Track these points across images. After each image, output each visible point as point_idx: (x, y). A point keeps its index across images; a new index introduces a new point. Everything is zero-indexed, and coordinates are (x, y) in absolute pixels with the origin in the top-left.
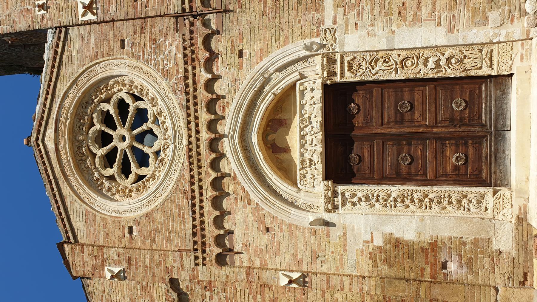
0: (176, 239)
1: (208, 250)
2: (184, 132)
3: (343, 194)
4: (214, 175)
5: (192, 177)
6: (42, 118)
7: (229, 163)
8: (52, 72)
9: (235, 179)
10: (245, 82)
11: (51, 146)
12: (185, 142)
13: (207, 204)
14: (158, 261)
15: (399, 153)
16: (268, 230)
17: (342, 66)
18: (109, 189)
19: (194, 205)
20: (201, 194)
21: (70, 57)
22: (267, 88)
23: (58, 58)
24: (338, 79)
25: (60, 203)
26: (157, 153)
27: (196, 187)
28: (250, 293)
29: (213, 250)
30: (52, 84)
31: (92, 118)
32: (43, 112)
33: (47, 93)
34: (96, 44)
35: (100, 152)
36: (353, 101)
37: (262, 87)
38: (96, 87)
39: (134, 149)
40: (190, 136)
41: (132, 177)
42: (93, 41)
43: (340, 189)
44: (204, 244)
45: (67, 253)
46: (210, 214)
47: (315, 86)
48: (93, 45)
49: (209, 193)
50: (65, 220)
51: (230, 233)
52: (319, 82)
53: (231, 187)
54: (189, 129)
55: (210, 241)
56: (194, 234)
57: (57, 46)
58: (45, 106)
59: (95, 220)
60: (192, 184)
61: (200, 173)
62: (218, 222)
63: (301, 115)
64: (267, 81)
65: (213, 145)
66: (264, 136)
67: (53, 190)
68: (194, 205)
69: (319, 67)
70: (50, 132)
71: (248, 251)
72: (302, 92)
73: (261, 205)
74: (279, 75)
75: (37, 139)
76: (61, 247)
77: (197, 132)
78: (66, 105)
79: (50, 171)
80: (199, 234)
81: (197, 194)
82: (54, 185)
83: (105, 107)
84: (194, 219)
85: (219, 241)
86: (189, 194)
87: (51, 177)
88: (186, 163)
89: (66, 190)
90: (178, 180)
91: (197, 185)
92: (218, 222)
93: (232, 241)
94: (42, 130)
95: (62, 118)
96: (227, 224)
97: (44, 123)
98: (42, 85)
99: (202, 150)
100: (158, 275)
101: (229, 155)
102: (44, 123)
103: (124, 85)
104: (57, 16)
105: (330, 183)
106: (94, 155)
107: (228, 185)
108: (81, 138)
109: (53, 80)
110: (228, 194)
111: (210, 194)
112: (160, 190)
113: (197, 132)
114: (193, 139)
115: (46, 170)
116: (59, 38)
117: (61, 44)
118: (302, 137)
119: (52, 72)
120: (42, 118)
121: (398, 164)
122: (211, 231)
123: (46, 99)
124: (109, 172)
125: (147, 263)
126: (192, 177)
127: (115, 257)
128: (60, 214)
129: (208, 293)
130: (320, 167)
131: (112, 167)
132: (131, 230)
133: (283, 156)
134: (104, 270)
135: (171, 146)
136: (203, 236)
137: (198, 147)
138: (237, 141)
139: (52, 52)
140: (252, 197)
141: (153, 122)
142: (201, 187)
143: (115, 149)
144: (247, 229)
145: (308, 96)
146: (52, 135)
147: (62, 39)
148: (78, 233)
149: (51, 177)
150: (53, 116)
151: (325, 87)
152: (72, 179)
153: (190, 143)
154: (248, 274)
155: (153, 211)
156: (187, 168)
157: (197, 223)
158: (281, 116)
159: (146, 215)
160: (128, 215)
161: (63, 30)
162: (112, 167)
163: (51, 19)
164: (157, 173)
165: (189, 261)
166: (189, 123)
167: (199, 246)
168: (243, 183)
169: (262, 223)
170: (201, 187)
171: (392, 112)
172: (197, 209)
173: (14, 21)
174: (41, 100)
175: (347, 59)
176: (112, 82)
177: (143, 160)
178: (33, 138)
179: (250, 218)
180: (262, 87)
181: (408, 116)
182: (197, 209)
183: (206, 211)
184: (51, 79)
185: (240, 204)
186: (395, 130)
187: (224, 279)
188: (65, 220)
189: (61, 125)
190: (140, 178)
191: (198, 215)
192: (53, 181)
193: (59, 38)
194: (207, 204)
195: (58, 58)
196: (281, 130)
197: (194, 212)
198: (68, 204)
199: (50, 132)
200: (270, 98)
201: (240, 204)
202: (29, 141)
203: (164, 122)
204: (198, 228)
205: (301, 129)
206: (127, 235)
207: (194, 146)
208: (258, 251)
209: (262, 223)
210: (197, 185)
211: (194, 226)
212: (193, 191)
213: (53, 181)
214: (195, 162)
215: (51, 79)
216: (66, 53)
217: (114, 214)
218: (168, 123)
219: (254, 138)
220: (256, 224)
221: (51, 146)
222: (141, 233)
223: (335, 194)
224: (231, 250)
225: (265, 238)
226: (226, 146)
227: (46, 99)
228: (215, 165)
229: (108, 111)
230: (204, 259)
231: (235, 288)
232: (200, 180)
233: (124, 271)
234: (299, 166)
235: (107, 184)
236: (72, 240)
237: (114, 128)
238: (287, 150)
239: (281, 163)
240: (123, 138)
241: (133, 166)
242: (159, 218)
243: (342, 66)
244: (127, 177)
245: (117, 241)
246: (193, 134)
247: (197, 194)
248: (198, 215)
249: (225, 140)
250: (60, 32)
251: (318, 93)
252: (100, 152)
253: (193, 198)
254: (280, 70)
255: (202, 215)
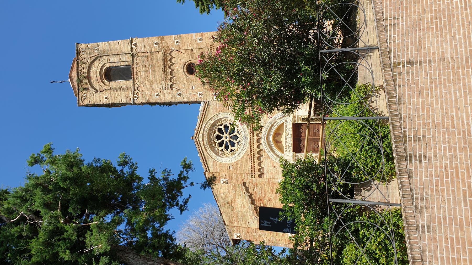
0: (245, 170)
1: (256, 173)
2: (249, 136)
3: (298, 156)
4: (258, 150)
5: (251, 150)
6: (198, 130)
7: (263, 146)
8: (203, 115)
9: (265, 151)
10: (269, 122)
11: (201, 139)
12: (249, 139)
13: (256, 159)
14: (239, 177)
15: (315, 144)
16: (275, 167)
17: (298, 119)
18: (221, 154)
19: (251, 159)
20: (254, 156)
21: (209, 111)
22: (275, 124)
23: (205, 111)
24: (297, 122)
25: (204, 159)
26: (238, 143)
27: (252, 154)
28: (269, 186)
29: (258, 173)
30: (202, 119)
31: (215, 131)
32: (199, 128)
33: (200, 122)
34: (219, 107)
35: (218, 142)
36: (301, 128)
37: (274, 123)
38: (218, 121)
39: (230, 141)
40: (251, 138)
41: (229, 150)
42: (218, 106)
43: (297, 154)
44: (254, 171)
45: (207, 175)
46: (257, 162)
47: (290, 124)
48: (218, 108)
49: (257, 155)
50: (206, 164)
51: (263, 168)
52: (291, 123)
53: (263, 154)
54: (251, 136)
55: (256, 170)
56: (252, 168)
57: (205, 107)
58: (199, 126)
59: (217, 164)
60: (251, 152)
61: (253, 149)
62: (259, 164)
63: (286, 132)
64: (275, 122)
65: (258, 141)
66: (274, 138)
67: (201, 154)
68: (251, 159)
69: (291, 119)
70: (201, 135)
71: (269, 173)
72: (286, 126)
73: (273, 159)
74: (279, 120)
75: (196, 137)
76: (205, 173)
77: (253, 137)
78: (207, 126)
79: (200, 148)
80: (253, 168)
81: (252, 156)
82: (202, 153)
83: (220, 127)
84: (251, 164)
85: (259, 170)
86: (250, 156)
87: (201, 150)
88: (249, 146)
89: (206, 154)
90: (246, 151)
91: (252, 153)
92: (259, 164)
93: (263, 171)
94: (198, 134)
95: (206, 130)
96: (262, 165)
97: (199, 132)
98: (198, 120)
99: (254, 142)
100: (239, 182)
101: (263, 144)
102: (199, 132)
103: (228, 121)
104: (206, 98)
105: (294, 153)
106: (215, 143)
107: (263, 153)
108: (211, 137)
109: (203, 118)
110: (263, 156)
111: (257, 156)
112: (240, 154)
113: (253, 137)
114: (252, 139)
115: (199, 148)
116: (206, 105)
117: (206, 106)
118: (286, 139)
119: (203, 115)
120: (198, 130)
121: (314, 147)
122: (257, 167)
123: (200, 124)
124: (221, 148)
125: (235, 178)
126: (251, 150)
127: (224, 176)
128: (204, 162)
129: (255, 187)
130: (291, 148)
131: (222, 147)
132: (229, 167)
133: (280, 144)
134: (220, 180)
135: (244, 141)
136: (254, 169)
137: (253, 141)
138: (265, 140)
139: (203, 109)
140: (270, 157)
141: (237, 133)
142: (254, 154)
143: (223, 141)
144: (268, 166)
145: (288, 127)
146: (202, 136)
147: (207, 105)
148: (210, 169)
149: (201, 150)
150: (202, 130)
151: (293, 124)
152: (208, 151)
153: (251, 140)
154: (269, 180)
155: (238, 161)
156: (249, 147)
157: (252, 165)
158: (279, 132)
159: (235, 162)
160: (229, 162)
161: (207, 102)
162: (222, 147)
163: (203, 98)
164: (238, 149)
165: (249, 177)
166: (250, 134)
167: (253, 172)
168: (267, 153)
169: (273, 165)
170: (254, 154)
171: (313, 132)
172: (253, 160)
173: (189, 98)
174: (198, 124)
175: (299, 117)
176: (223, 119)
177: (233, 145)
178: (194, 137)
179: (270, 163)
180: (274, 123)
181: (317, 133)
182: (253, 160)
183: (255, 161)
184: (202, 118)
185: (266, 159)
186: (313, 137)
187: (261, 182)
188: (206, 164)
189: (205, 133)
190: (232, 150)
191: (253, 162)
192: (202, 151)
193: (206, 105)
194: (256, 159)
195: (205, 111)
196: (279, 136)
197: (251, 161)
198: (207, 159)
199: (201, 135)
200: (276, 127)
201: (266, 159)
202: (193, 138)
203: (241, 133)
204: (253, 166)
205: (286, 137)
206: (228, 169)
207: (252, 141)
208: (272, 173)
209: (273, 165)
210: (252, 153)
211: (252, 166)
212: (251, 155)
213: (202, 151)
214: (252, 146)
215: (202, 118)
216: (208, 110)
217: (223, 162)
218: (243, 133)
219: (271, 139)
220: (271, 165)
221: (201, 139)
222: (233, 168)
223: (296, 156)
224: (263, 173)
225: (274, 169)
226: (262, 141)
227: (200, 124)
228: (258, 147)
229: (221, 128)
230: (255, 176)
231: (264, 185)
232: (254, 151)
233: (227, 181)
234: (285, 147)
235: (220, 152)
236: (208, 171)
237: (223, 134)
238: (281, 142)
239: (279, 146)
240: (226, 138)
241: (230, 146)
242: (240, 163)
243: (298, 119)
244: (227, 150)
245: (225, 171)
246: (252, 137)
247: (252, 156)
248: (253, 162)
249: (262, 139)
250: (206, 103)
251: (291, 126)
252: (218, 142)
253: (251, 157)
254: (279, 119)
255: (254, 162)
